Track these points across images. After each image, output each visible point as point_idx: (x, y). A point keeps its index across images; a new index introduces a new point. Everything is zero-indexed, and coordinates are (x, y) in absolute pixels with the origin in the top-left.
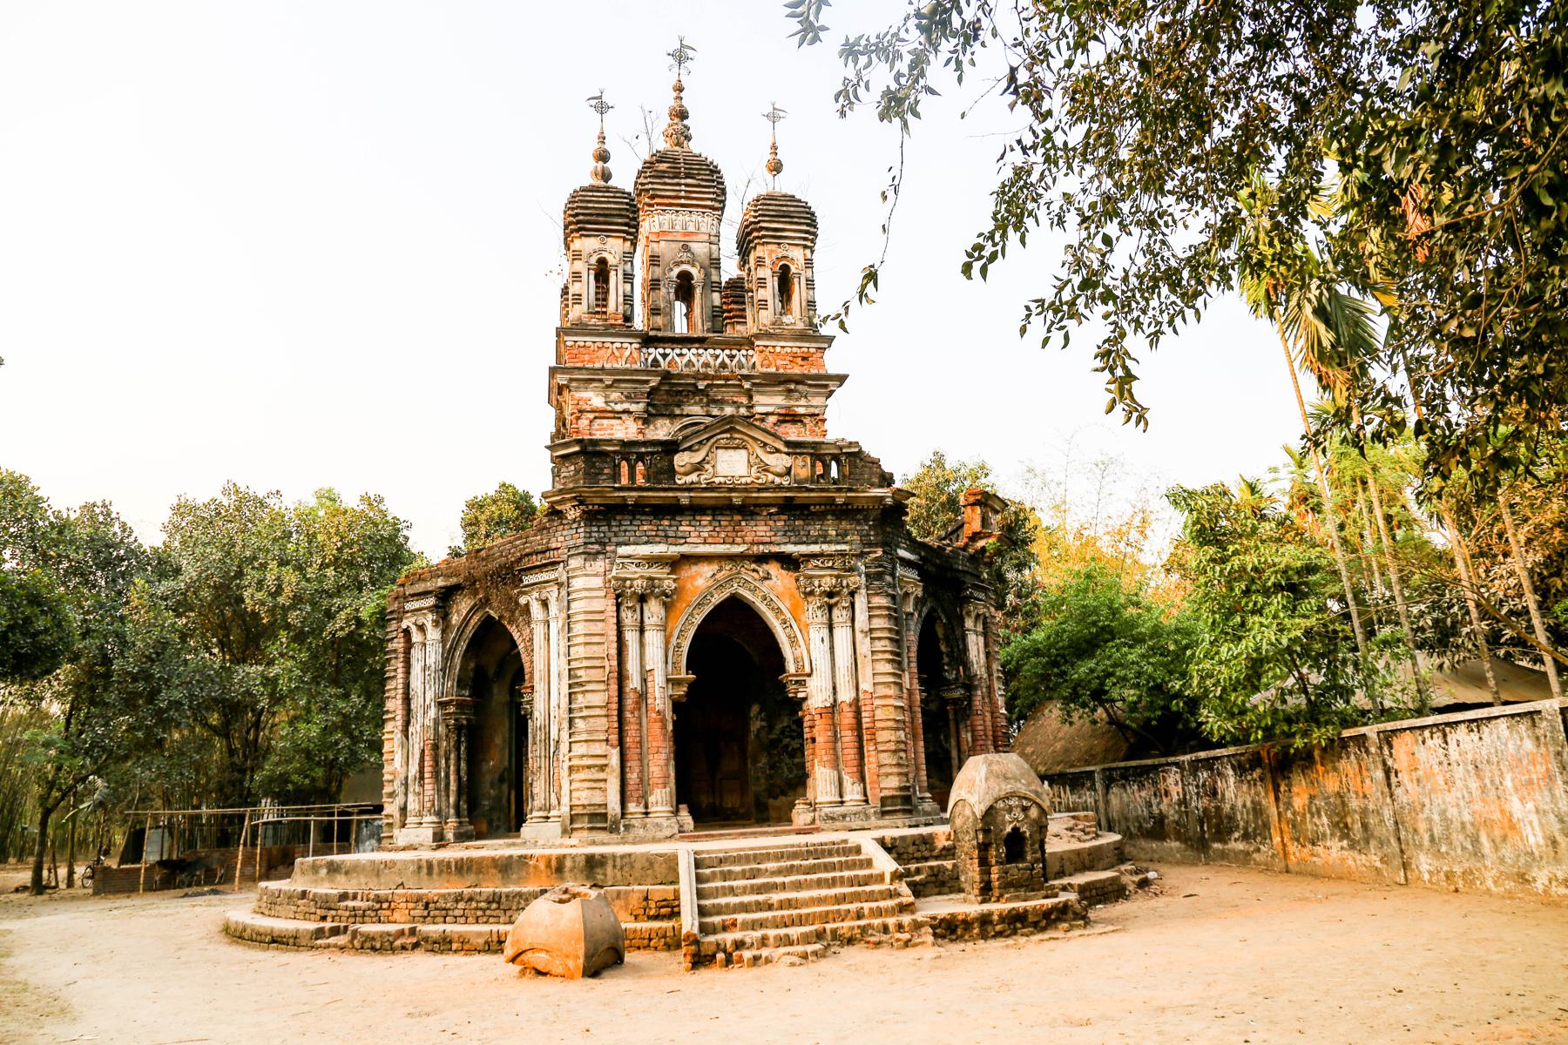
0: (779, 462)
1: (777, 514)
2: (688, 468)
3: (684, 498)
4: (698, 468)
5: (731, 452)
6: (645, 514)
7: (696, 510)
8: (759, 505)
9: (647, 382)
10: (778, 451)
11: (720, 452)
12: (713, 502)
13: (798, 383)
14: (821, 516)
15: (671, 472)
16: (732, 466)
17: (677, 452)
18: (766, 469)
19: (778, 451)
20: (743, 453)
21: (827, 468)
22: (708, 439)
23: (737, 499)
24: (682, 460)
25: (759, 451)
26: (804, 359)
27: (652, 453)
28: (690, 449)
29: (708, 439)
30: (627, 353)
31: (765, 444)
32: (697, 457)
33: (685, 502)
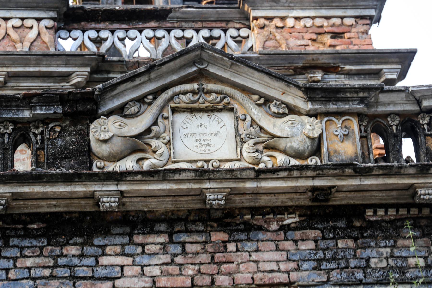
0: (297, 131)
1: (299, 227)
2: (117, 145)
3: (108, 195)
4: (138, 144)
5: (203, 118)
6: (28, 234)
7: (133, 223)
8: (255, 211)
9: (66, 77)
10: (292, 110)
11: (180, 118)
12: (167, 205)
13: (327, 70)
14: (391, 230)
15: (86, 153)
16: (205, 140)
17: (94, 116)
18: (271, 144)
19: (292, 110)
20: (226, 119)
21: (393, 148)
22: (156, 94)
23: (215, 193)
24: (105, 131)
25: (257, 114)
26: (336, 35)
27: (45, 121)
28: (120, 111)
29: (156, 94)
30: (32, 35)
31: (268, 101)
32: (136, 126)
33: (109, 203)
